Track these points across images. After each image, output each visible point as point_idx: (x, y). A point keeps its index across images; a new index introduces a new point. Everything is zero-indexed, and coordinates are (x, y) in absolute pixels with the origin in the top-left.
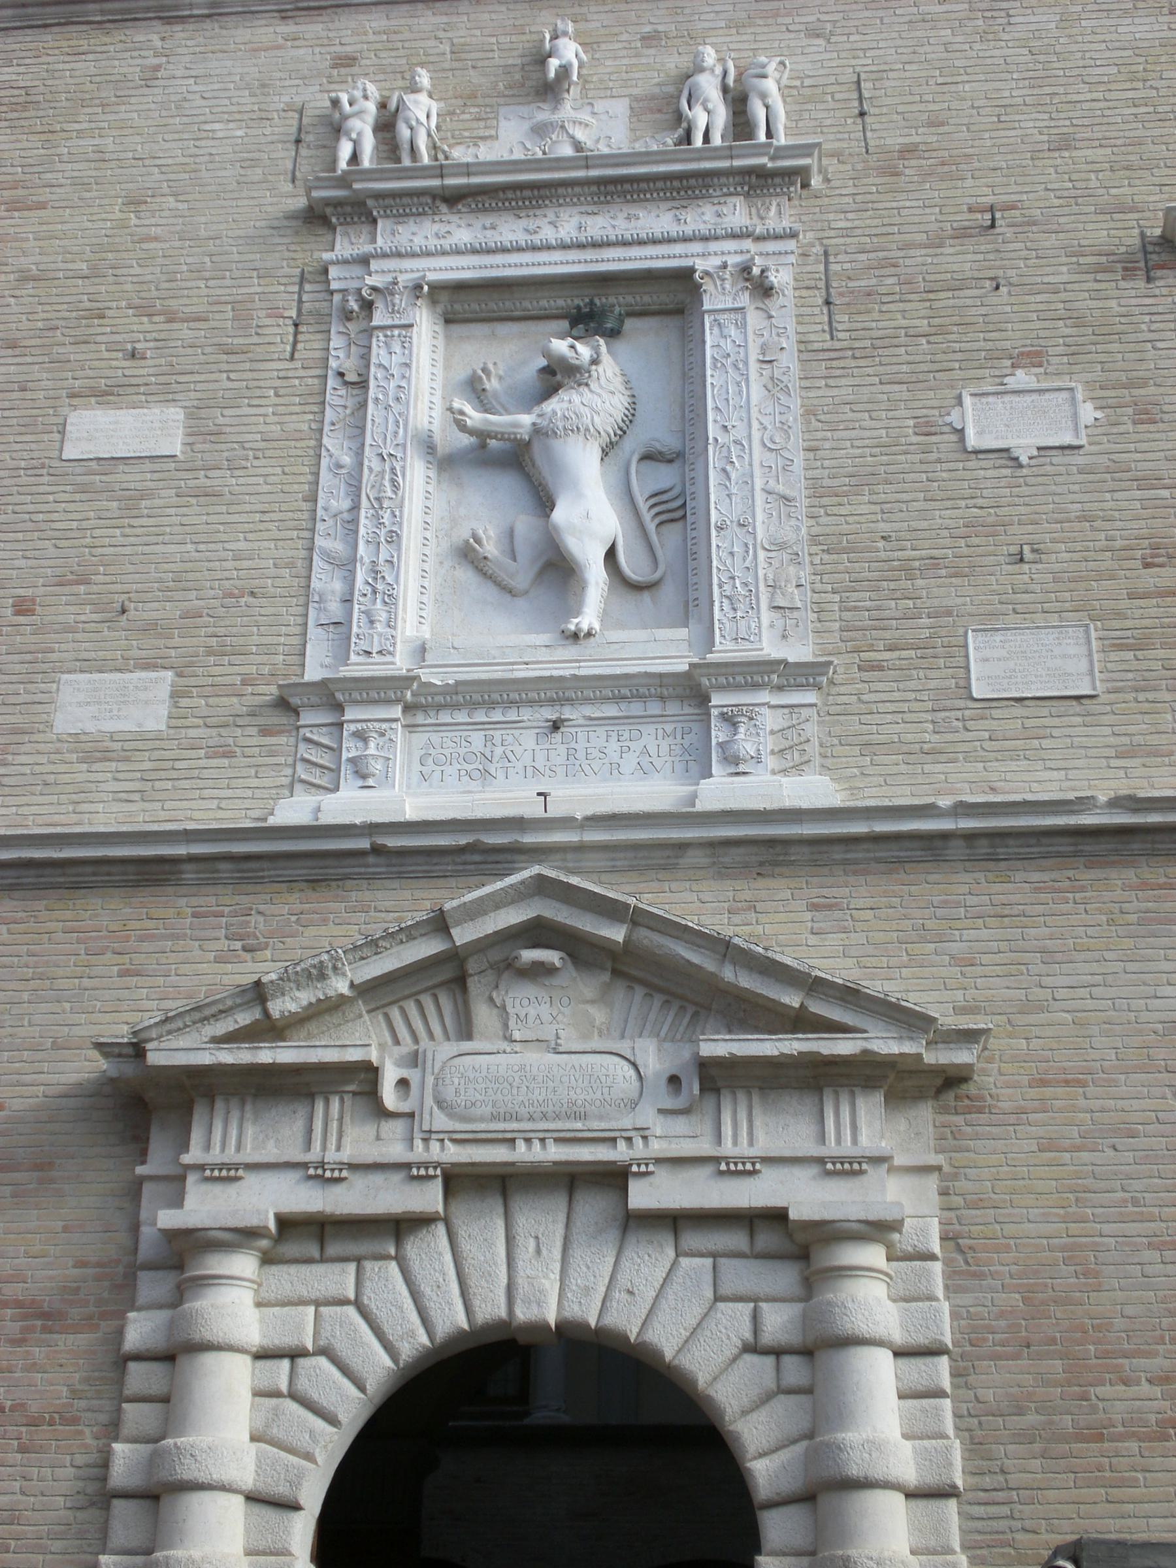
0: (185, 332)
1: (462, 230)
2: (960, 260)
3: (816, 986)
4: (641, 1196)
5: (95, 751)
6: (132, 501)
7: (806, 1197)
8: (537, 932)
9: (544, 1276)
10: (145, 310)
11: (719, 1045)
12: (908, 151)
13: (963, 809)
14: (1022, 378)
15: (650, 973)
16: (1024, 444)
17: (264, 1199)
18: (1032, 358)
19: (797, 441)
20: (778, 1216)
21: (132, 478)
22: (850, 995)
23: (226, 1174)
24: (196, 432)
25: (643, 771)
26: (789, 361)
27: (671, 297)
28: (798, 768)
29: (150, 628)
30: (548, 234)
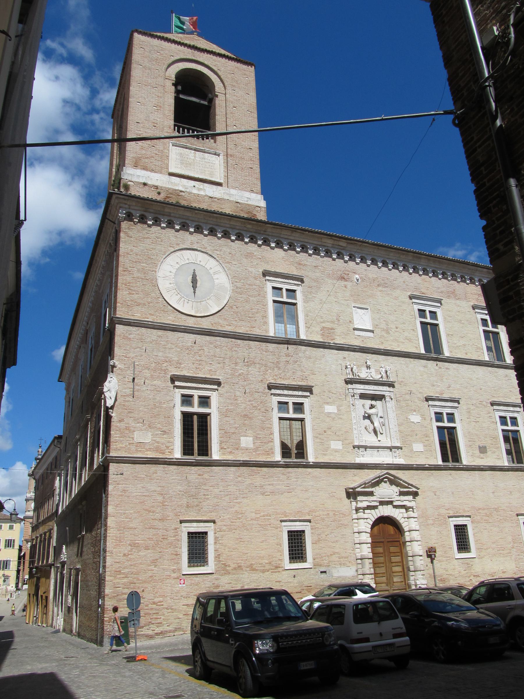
0: (335, 395)
1: (362, 386)
2: (408, 397)
3: (409, 484)
4: (395, 504)
5: (336, 451)
6: (334, 418)
7: (408, 504)
8: (386, 478)
9: (387, 511)
10: (329, 392)
11: (402, 490)
12: (402, 381)
13: (416, 465)
14: (414, 413)
15: (394, 482)
16: (415, 421)
17: (365, 504)
18: (415, 411)
19: (396, 418)
20: (404, 505)
21: (333, 416)
22: (412, 485)
23: (361, 501)
24: (338, 410)
25: (386, 457)
26: (394, 408)
27: (380, 398)
28: (400, 458)
29: (338, 436)
30: (370, 388)
